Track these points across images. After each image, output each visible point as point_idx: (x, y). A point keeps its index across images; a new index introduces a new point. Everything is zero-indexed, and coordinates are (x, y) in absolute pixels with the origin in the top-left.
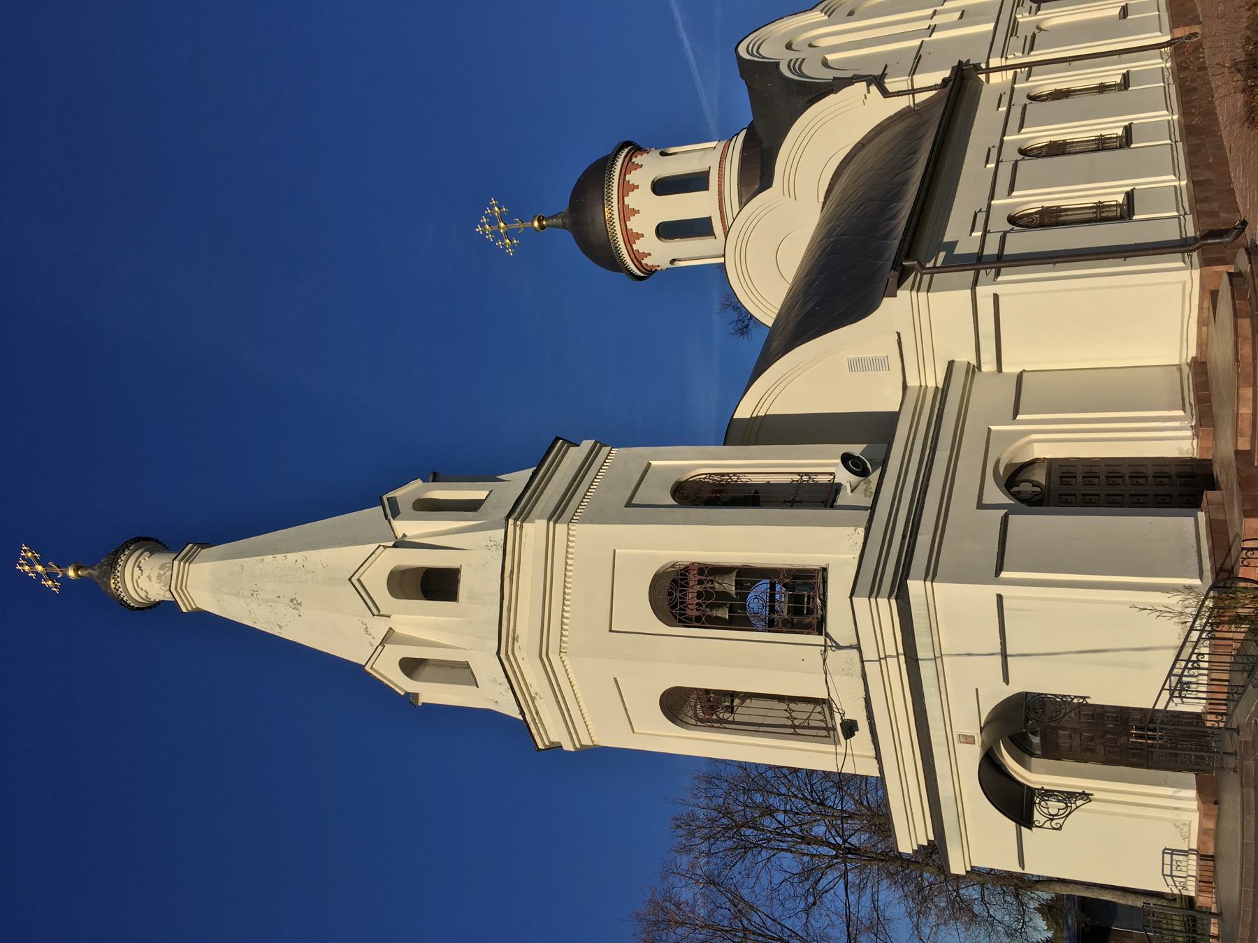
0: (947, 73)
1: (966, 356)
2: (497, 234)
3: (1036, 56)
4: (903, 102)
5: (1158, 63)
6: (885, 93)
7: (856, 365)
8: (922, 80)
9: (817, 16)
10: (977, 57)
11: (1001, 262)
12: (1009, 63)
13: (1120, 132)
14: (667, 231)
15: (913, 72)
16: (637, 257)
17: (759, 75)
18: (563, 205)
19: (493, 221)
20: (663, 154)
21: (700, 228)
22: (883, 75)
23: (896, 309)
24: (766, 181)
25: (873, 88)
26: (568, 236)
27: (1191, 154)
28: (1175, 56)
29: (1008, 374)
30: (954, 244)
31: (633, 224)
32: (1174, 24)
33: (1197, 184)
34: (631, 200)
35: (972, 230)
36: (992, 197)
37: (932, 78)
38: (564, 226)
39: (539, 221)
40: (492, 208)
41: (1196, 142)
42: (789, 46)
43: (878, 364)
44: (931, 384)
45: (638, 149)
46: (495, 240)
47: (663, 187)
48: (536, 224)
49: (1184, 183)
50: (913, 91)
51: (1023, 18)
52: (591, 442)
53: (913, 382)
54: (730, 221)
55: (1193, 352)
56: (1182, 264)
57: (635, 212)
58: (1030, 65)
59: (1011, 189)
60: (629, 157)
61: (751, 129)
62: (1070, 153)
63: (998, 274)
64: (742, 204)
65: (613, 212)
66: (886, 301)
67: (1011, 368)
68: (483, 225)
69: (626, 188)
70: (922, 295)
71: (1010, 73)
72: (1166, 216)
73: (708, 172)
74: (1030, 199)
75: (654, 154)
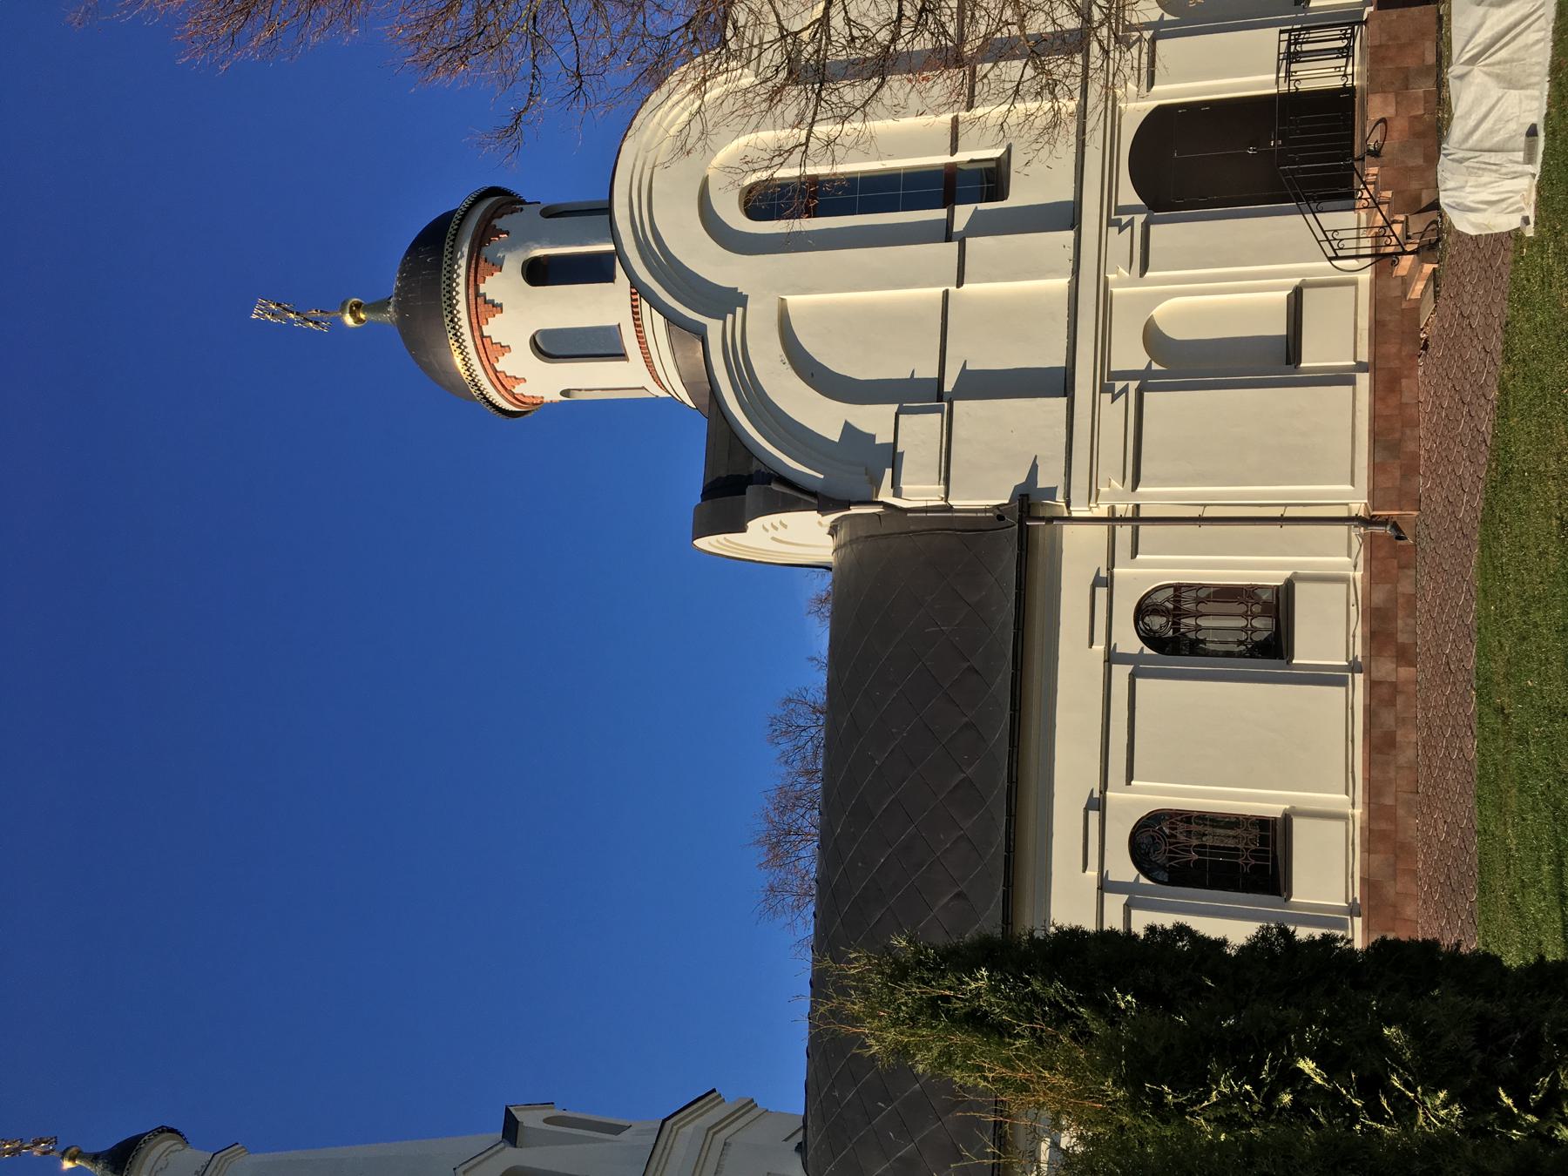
5: (1341, 557)
22: (893, 457)
28: (1371, 544)
47: (550, 347)
51: (1123, 283)
60: (474, 281)
62: (1207, 654)
71: (1103, 529)
73: (613, 333)
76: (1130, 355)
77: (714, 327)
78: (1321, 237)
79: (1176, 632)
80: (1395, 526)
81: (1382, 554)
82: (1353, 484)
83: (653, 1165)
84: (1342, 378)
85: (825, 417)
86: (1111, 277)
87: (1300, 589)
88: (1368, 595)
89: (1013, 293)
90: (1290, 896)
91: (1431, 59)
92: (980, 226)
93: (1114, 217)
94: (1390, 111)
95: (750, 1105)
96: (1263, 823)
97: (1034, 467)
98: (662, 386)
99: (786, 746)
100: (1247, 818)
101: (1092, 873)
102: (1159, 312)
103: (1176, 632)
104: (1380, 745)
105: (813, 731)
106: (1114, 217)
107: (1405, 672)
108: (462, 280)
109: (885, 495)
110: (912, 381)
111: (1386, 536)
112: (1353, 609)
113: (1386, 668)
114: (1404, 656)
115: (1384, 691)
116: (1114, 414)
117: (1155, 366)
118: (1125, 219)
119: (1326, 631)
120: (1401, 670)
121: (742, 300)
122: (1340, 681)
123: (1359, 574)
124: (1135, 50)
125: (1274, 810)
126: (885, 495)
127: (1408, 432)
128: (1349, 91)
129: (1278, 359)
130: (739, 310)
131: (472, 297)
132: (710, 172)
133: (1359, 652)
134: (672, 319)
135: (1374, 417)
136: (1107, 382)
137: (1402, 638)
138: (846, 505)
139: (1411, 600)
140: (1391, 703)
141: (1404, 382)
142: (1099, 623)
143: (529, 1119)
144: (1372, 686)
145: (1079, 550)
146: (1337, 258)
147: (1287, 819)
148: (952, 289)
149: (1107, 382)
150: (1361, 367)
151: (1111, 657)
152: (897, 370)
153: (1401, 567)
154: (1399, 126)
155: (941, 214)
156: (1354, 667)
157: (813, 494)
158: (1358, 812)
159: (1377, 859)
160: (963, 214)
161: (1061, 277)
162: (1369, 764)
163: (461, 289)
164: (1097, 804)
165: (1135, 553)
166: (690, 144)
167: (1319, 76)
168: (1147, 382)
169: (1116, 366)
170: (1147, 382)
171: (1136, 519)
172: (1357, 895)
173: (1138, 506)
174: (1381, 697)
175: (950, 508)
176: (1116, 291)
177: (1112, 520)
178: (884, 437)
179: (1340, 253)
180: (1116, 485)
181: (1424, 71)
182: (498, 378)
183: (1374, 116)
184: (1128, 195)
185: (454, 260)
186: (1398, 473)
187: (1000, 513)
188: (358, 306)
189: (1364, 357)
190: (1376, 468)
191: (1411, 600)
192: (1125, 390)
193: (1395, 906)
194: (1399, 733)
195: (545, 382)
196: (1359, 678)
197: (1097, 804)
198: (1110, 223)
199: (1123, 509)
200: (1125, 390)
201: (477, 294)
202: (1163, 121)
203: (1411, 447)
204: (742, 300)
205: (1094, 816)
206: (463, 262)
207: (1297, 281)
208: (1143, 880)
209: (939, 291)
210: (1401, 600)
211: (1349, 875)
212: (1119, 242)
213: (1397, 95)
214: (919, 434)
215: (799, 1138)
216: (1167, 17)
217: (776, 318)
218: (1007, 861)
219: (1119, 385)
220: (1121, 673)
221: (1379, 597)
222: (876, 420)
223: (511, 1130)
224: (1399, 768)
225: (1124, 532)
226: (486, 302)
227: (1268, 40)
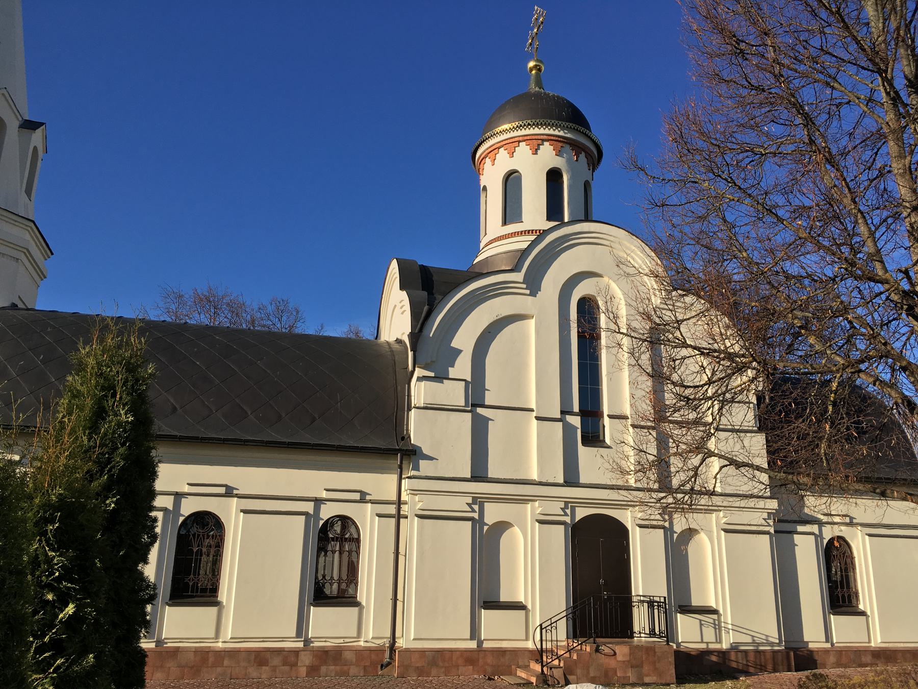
22: (441, 377)
28: (379, 650)
47: (512, 181)
51: (531, 510)
62: (318, 557)
71: (394, 497)
76: (493, 513)
77: (519, 277)
78: (553, 620)
79: (333, 540)
80: (389, 664)
81: (373, 656)
82: (414, 639)
83: (5, 213)
84: (474, 632)
85: (465, 339)
86: (537, 504)
87: (355, 610)
88: (350, 649)
89: (530, 447)
90: (170, 605)
91: (647, 680)
92: (568, 430)
93: (569, 505)
94: (620, 657)
95: (43, 276)
96: (214, 590)
97: (431, 458)
98: (486, 245)
99: (270, 309)
100: (218, 581)
101: (187, 489)
102: (516, 530)
103: (333, 540)
104: (260, 657)
105: (279, 325)
106: (569, 505)
107: (303, 671)
108: (551, 132)
109: (419, 372)
110: (484, 390)
111: (384, 658)
112: (341, 641)
113: (306, 660)
114: (313, 670)
115: (292, 659)
116: (460, 504)
117: (486, 528)
118: (568, 511)
119: (329, 625)
120: (305, 669)
121: (533, 294)
122: (299, 633)
123: (362, 644)
124: (658, 517)
125: (223, 596)
126: (419, 372)
127: (443, 670)
128: (633, 637)
129: (487, 597)
130: (528, 292)
131: (542, 137)
132: (606, 279)
133: (316, 644)
134: (525, 253)
135: (451, 651)
136: (479, 501)
137: (323, 669)
138: (414, 349)
139: (346, 674)
140: (285, 663)
141: (471, 667)
142: (338, 495)
143: (37, 137)
144: (296, 652)
145: (382, 484)
146: (541, 629)
147: (216, 604)
148: (534, 414)
149: (479, 501)
150: (480, 643)
151: (318, 502)
152: (490, 381)
153: (365, 667)
154: (612, 663)
155: (576, 409)
156: (307, 642)
157: (421, 330)
158: (220, 645)
159: (191, 656)
160: (576, 421)
161: (538, 476)
162: (249, 651)
163: (547, 131)
164: (229, 492)
165: (379, 516)
166: (621, 268)
167: (640, 619)
168: (477, 523)
169: (487, 506)
170: (477, 523)
171: (399, 517)
172: (169, 645)
173: (407, 517)
174: (289, 657)
175: (409, 409)
176: (529, 506)
177: (399, 503)
178: (452, 372)
179: (544, 631)
180: (419, 505)
181: (641, 676)
182: (495, 149)
183: (618, 649)
184: (581, 513)
185: (563, 128)
186: (419, 665)
187: (406, 438)
188: (540, 70)
189: (486, 645)
190: (422, 652)
191: (346, 674)
192: (473, 511)
193: (162, 666)
194: (267, 668)
195: (492, 177)
196: (301, 645)
197: (229, 492)
198: (566, 503)
199: (405, 509)
200: (473, 511)
201: (543, 140)
202: (619, 532)
203: (434, 672)
204: (533, 294)
205: (222, 490)
206: (561, 133)
207: (529, 607)
208: (181, 519)
209: (533, 406)
210: (346, 668)
211: (181, 640)
212: (555, 508)
213: (628, 661)
214: (453, 393)
215: (20, 305)
216: (675, 536)
217: (522, 312)
218: (197, 438)
219: (476, 507)
220: (309, 507)
221: (348, 655)
222: (462, 368)
223: (30, 126)
224: (246, 668)
225: (392, 509)
226: (539, 145)
227: (660, 590)
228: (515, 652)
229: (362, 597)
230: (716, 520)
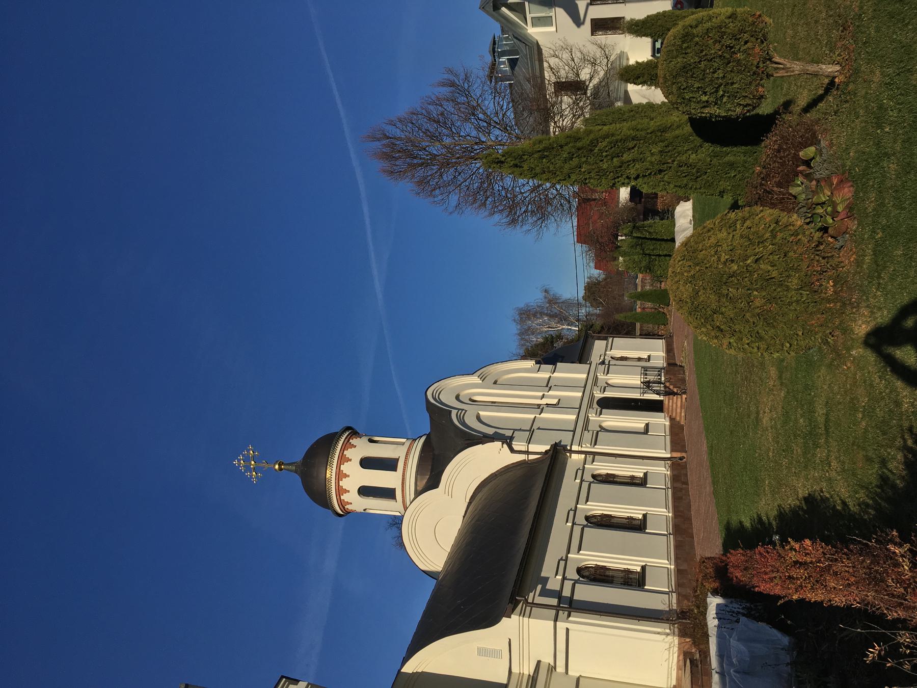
0: (548, 447)
1: (548, 659)
2: (247, 468)
3: (598, 449)
4: (522, 457)
5: (662, 471)
6: (512, 451)
7: (482, 652)
8: (533, 448)
9: (475, 379)
10: (565, 439)
11: (571, 606)
12: (583, 449)
13: (641, 475)
14: (365, 491)
15: (529, 442)
16: (342, 504)
17: (439, 414)
18: (299, 457)
19: (247, 459)
20: (371, 441)
21: (388, 494)
23: (509, 625)
24: (433, 483)
25: (505, 446)
26: (297, 479)
27: (677, 547)
29: (572, 676)
30: (546, 579)
31: (344, 483)
32: (672, 451)
33: (679, 572)
34: (345, 468)
35: (556, 574)
36: (568, 552)
37: (540, 448)
38: (296, 472)
39: (279, 465)
40: (248, 451)
41: (680, 539)
42: (457, 398)
43: (495, 654)
44: (526, 673)
45: (355, 433)
46: (246, 471)
47: (367, 463)
48: (277, 467)
49: (673, 567)
50: (527, 453)
51: (592, 417)
52: (306, 683)
53: (515, 670)
54: (408, 503)
55: (674, 683)
56: (668, 631)
57: (346, 476)
58: (594, 454)
59: (580, 549)
61: (428, 436)
63: (569, 616)
64: (418, 493)
65: (331, 473)
66: (504, 618)
67: (574, 672)
68: (239, 461)
69: (343, 459)
70: (526, 619)
71: (583, 456)
72: (660, 594)
73: (397, 460)
74: (591, 558)
75: (365, 440)
77: (454, 412)
85: (490, 431)
113: (679, 485)
116: (588, 436)
184: (595, 406)
209: (532, 416)
220: (585, 486)
221: (676, 473)
225: (590, 458)
228: (671, 427)
229: (641, 475)
230: (601, 376)
